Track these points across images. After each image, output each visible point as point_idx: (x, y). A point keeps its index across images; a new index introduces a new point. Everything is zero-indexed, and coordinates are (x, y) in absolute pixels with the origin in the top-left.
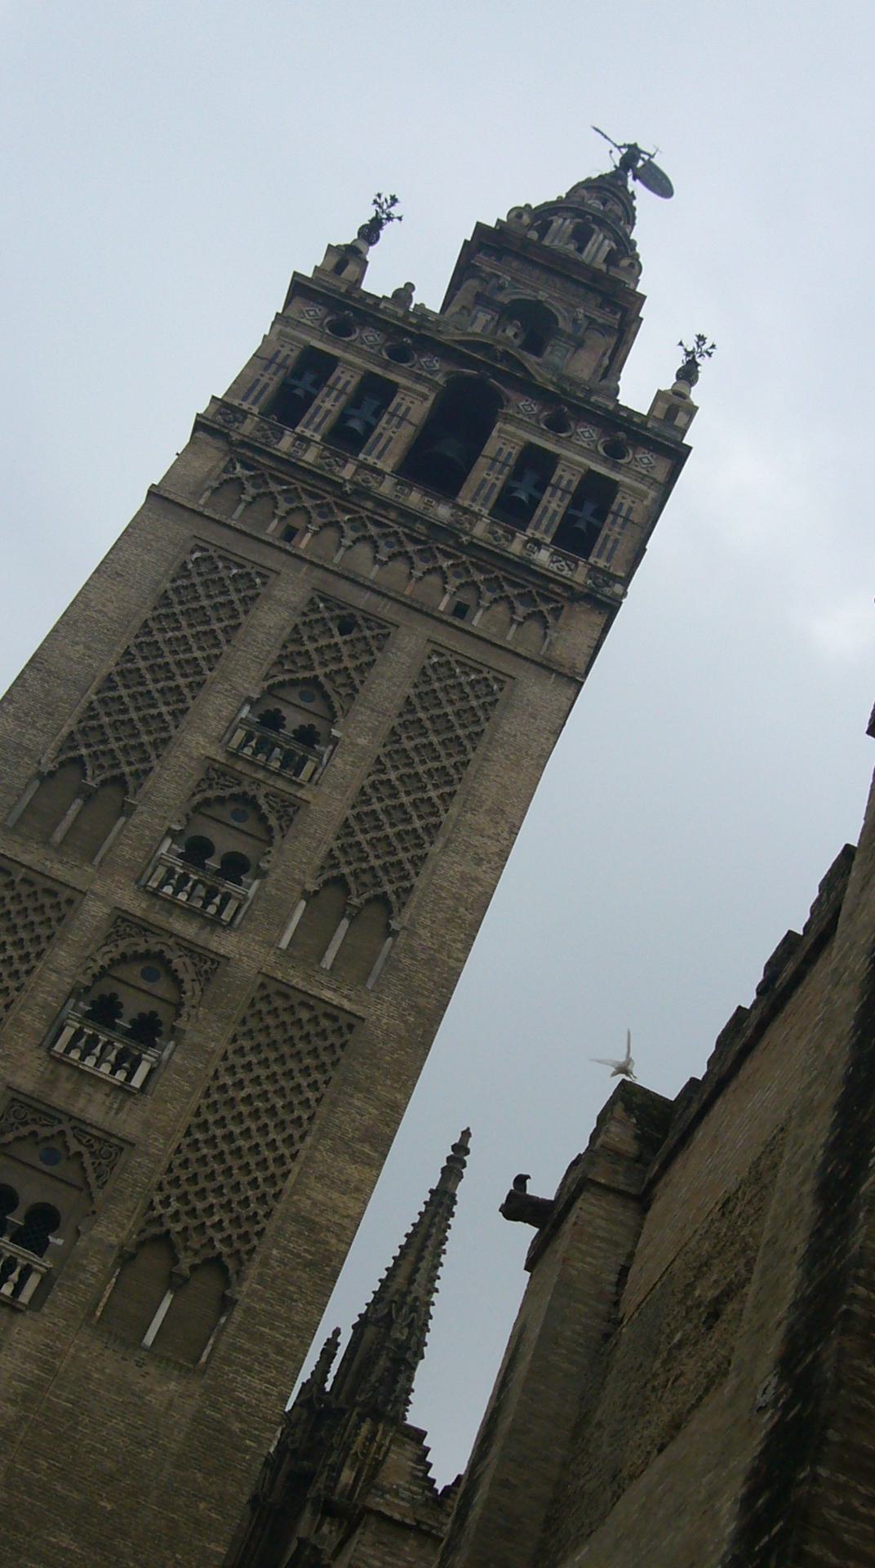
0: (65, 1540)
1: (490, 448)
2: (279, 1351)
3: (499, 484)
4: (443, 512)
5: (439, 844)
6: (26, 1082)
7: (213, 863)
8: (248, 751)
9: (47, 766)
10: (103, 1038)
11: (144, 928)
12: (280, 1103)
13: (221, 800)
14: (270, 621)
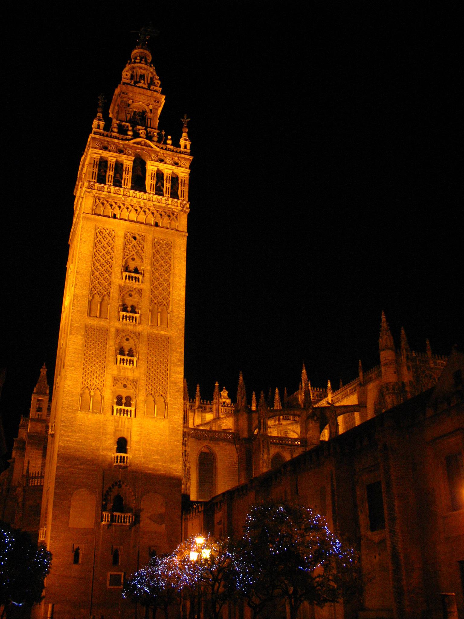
0: (156, 457)
1: (148, 174)
2: (178, 410)
3: (155, 184)
4: (145, 196)
5: (171, 287)
6: (115, 372)
7: (129, 309)
8: (127, 279)
9: (91, 298)
10: (125, 359)
11: (123, 331)
12: (161, 360)
13: (126, 293)
14: (119, 243)
